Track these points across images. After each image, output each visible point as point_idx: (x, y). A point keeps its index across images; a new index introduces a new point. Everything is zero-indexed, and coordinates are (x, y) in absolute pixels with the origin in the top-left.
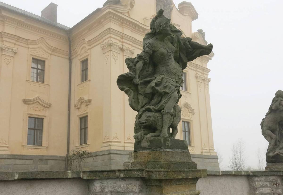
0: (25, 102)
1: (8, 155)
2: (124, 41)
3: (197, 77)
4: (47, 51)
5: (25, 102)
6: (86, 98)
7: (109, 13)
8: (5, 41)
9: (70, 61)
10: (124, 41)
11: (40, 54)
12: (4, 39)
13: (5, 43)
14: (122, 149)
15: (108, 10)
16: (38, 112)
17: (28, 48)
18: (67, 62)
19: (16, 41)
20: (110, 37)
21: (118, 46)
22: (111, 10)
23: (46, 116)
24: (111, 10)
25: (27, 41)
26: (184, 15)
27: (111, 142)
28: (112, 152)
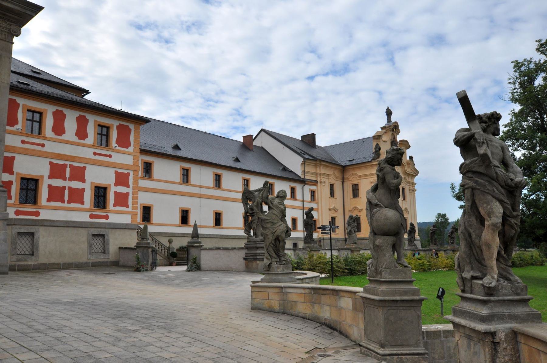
0: (330, 209)
3: (410, 190)
5: (330, 209)
6: (360, 208)
9: (343, 182)
11: (332, 181)
18: (341, 183)
25: (329, 175)
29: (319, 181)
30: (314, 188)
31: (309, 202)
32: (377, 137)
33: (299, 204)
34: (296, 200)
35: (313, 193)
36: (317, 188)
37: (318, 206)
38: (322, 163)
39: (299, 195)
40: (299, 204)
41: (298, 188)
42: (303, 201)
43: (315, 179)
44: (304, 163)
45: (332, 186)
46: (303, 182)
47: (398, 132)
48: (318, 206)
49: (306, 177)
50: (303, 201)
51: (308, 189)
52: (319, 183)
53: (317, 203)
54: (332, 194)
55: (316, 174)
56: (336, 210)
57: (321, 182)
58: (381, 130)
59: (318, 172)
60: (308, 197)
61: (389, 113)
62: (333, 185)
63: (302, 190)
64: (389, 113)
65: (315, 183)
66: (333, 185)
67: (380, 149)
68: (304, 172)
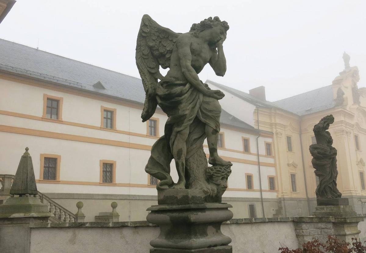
0: (288, 165)
1: (289, 198)
2: (347, 126)
4: (291, 130)
7: (341, 111)
8: (278, 128)
9: (300, 135)
10: (347, 126)
12: (277, 127)
13: (277, 129)
14: (355, 194)
15: (340, 109)
16: (293, 172)
17: (285, 130)
19: (281, 127)
20: (342, 126)
21: (346, 130)
22: (343, 109)
23: (296, 173)
24: (343, 109)
25: (284, 126)
26: (364, 97)
27: (351, 190)
28: (354, 197)
29: (274, 132)
30: (269, 140)
31: (265, 156)
32: (337, 82)
33: (254, 158)
34: (250, 154)
35: (268, 147)
36: (273, 141)
37: (275, 161)
38: (278, 112)
39: (253, 148)
40: (254, 158)
41: (252, 139)
42: (258, 155)
43: (269, 130)
44: (257, 112)
45: (289, 139)
46: (257, 133)
47: (358, 80)
48: (275, 161)
49: (260, 128)
50: (258, 155)
51: (262, 141)
52: (274, 135)
53: (274, 157)
54: (290, 148)
55: (271, 125)
56: (295, 166)
57: (277, 134)
58: (339, 75)
59: (273, 122)
60: (263, 151)
61: (346, 58)
62: (290, 138)
63: (255, 143)
64: (346, 58)
65: (270, 135)
66: (290, 138)
67: (343, 94)
68: (258, 122)
